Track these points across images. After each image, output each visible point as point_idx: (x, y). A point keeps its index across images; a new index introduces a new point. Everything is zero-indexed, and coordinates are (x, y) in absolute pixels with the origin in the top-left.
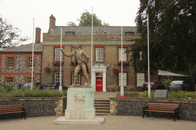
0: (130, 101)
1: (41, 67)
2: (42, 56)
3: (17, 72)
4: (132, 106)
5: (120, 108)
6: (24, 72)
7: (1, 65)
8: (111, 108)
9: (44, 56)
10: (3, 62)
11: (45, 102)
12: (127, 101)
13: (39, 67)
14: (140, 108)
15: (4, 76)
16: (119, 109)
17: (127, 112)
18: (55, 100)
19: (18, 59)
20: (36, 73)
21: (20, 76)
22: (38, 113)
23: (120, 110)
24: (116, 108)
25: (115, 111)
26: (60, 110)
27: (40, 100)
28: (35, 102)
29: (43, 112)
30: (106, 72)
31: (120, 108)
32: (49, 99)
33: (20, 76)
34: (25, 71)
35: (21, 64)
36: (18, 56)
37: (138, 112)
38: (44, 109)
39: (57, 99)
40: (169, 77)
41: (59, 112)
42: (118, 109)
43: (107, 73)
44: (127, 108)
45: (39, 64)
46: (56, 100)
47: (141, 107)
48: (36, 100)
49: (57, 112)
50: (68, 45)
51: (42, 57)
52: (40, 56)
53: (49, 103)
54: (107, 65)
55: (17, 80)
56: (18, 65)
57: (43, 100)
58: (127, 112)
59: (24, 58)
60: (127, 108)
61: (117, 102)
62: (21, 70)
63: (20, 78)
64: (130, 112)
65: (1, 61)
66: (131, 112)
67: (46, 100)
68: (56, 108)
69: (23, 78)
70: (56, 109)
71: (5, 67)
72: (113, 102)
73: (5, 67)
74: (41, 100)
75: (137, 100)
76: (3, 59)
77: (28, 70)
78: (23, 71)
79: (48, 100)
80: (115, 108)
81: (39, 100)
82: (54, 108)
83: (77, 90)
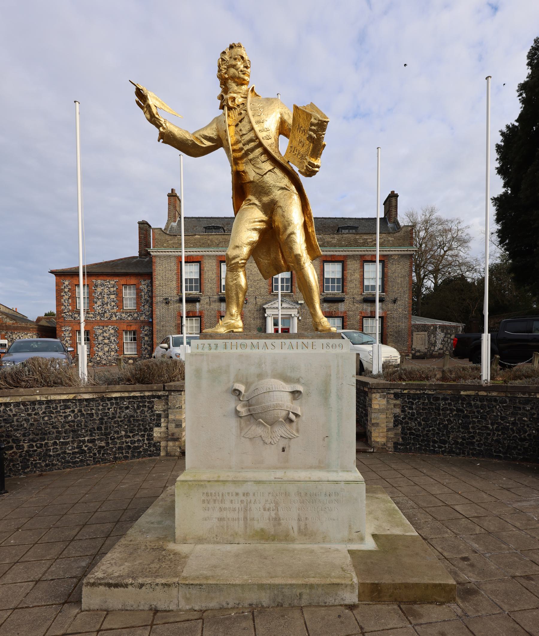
0: (457, 398)
1: (152, 308)
2: (152, 282)
3: (98, 318)
4: (466, 417)
5: (413, 424)
6: (114, 318)
7: (63, 305)
8: (377, 425)
9: (156, 283)
10: (67, 297)
11: (112, 404)
12: (445, 399)
13: (146, 307)
14: (507, 428)
15: (70, 328)
16: (410, 429)
17: (444, 442)
18: (154, 397)
19: (99, 290)
20: (142, 322)
21: (105, 328)
22: (82, 452)
23: (411, 434)
24: (397, 422)
25: (391, 434)
26: (173, 434)
27: (86, 396)
28: (67, 407)
29: (103, 444)
30: (298, 318)
31: (413, 424)
32: (126, 394)
33: (105, 328)
34: (116, 316)
35: (106, 300)
36: (99, 282)
37: (498, 441)
38: (106, 434)
39: (160, 393)
40: (432, 328)
41: (171, 444)
42: (403, 429)
43: (300, 318)
44: (446, 427)
45: (147, 301)
46: (159, 397)
47: (514, 423)
48: (71, 397)
49: (163, 444)
50: (209, 256)
51: (152, 286)
52: (148, 281)
53: (127, 408)
54: (300, 302)
55: (100, 338)
56: (99, 303)
57: (103, 399)
58: (444, 442)
59: (113, 287)
60: (446, 427)
61: (398, 402)
62: (107, 315)
63: (105, 331)
64: (456, 443)
65: (62, 294)
66: (460, 441)
67: (116, 398)
68: (158, 425)
69: (112, 331)
70: (157, 432)
71: (70, 308)
72: (384, 402)
73: (70, 308)
74: (93, 400)
75: (494, 394)
76: (66, 290)
77: (124, 315)
78: (111, 317)
79: (122, 398)
80: (391, 425)
81: (87, 400)
82: (151, 429)
83: (248, 351)
